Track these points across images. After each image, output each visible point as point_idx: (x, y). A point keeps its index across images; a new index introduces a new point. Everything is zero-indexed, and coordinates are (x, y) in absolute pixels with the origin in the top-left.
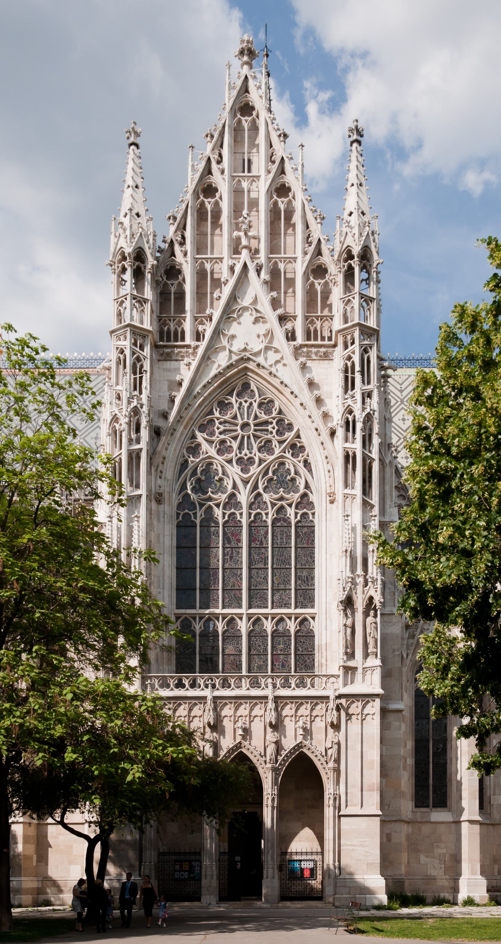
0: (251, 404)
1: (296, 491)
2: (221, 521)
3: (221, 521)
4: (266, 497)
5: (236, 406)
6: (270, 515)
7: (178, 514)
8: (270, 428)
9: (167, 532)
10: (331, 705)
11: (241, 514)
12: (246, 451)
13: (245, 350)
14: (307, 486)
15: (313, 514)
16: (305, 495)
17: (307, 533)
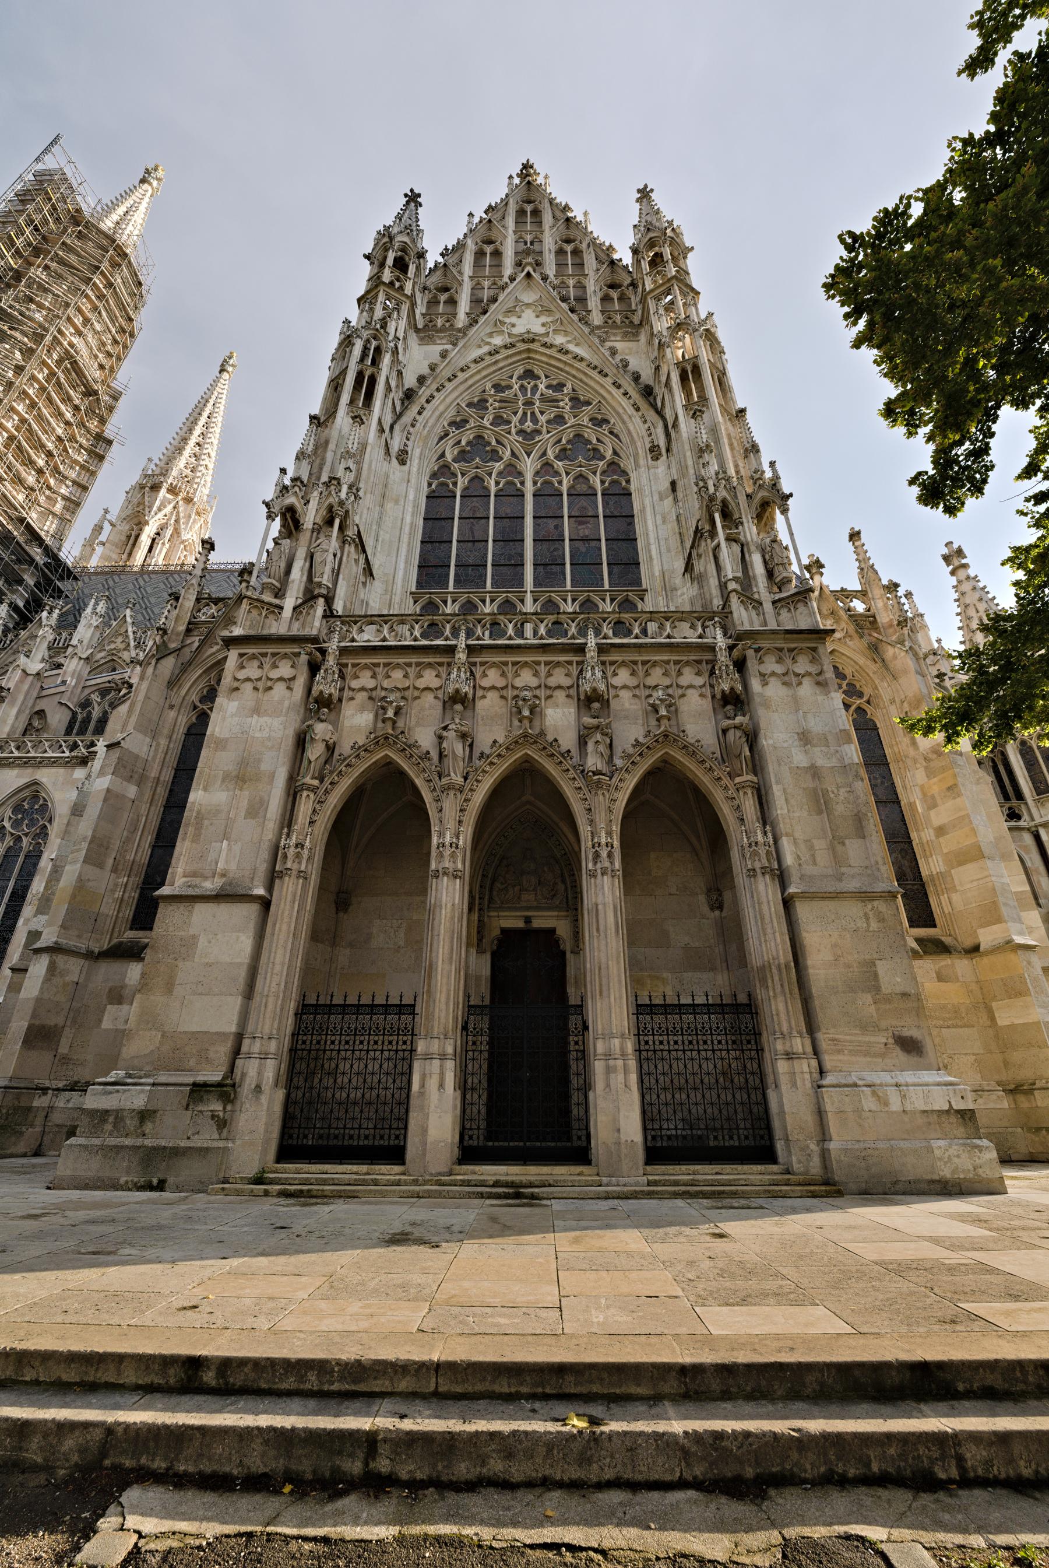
0: (536, 386)
1: (604, 458)
2: (493, 489)
3: (493, 489)
4: (559, 465)
5: (516, 387)
6: (565, 482)
7: (430, 485)
8: (561, 404)
9: (411, 497)
10: (723, 657)
11: (522, 483)
12: (529, 423)
13: (528, 332)
14: (615, 453)
15: (628, 481)
16: (612, 464)
17: (620, 495)
